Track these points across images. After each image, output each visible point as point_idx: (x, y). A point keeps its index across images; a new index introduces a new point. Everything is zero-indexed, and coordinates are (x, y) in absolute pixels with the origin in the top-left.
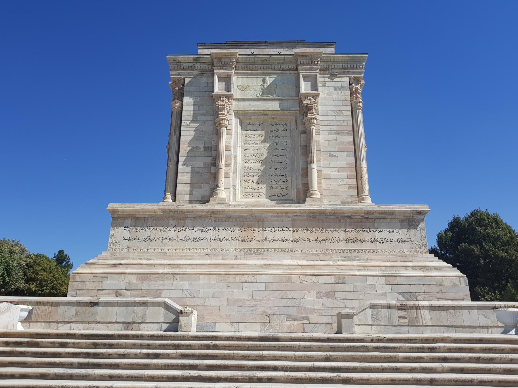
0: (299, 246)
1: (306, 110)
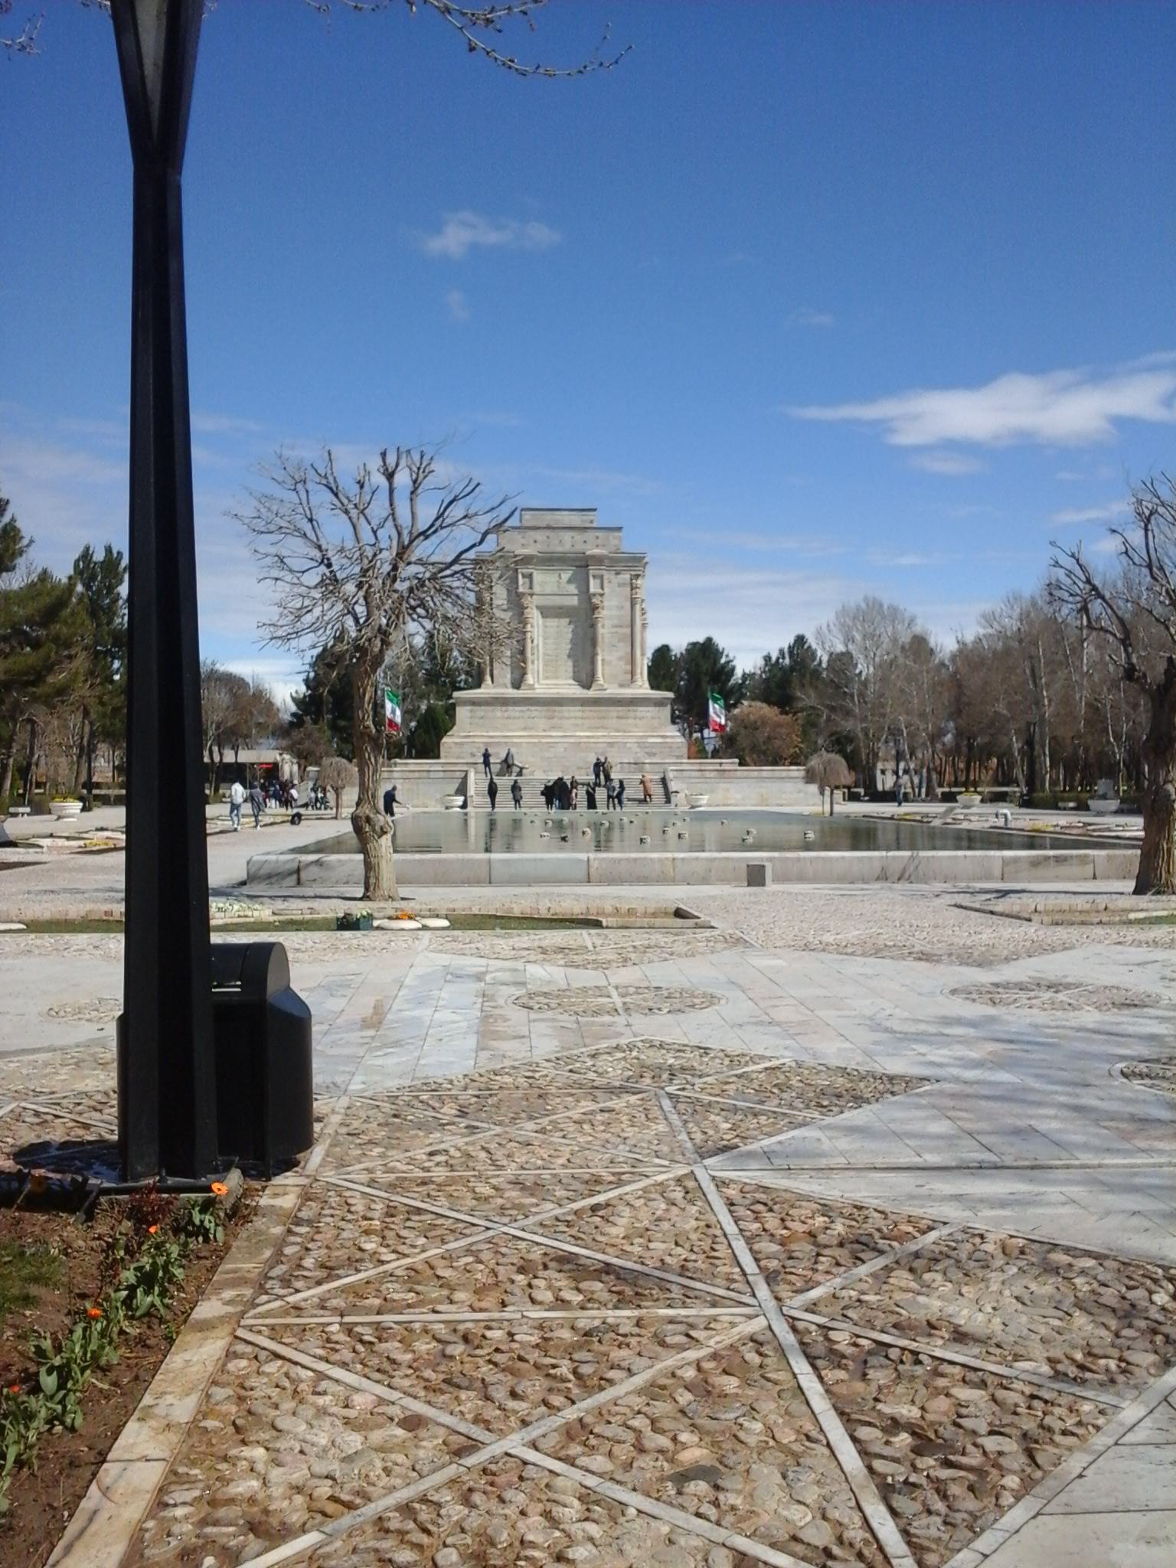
0: (587, 722)
1: (594, 608)
